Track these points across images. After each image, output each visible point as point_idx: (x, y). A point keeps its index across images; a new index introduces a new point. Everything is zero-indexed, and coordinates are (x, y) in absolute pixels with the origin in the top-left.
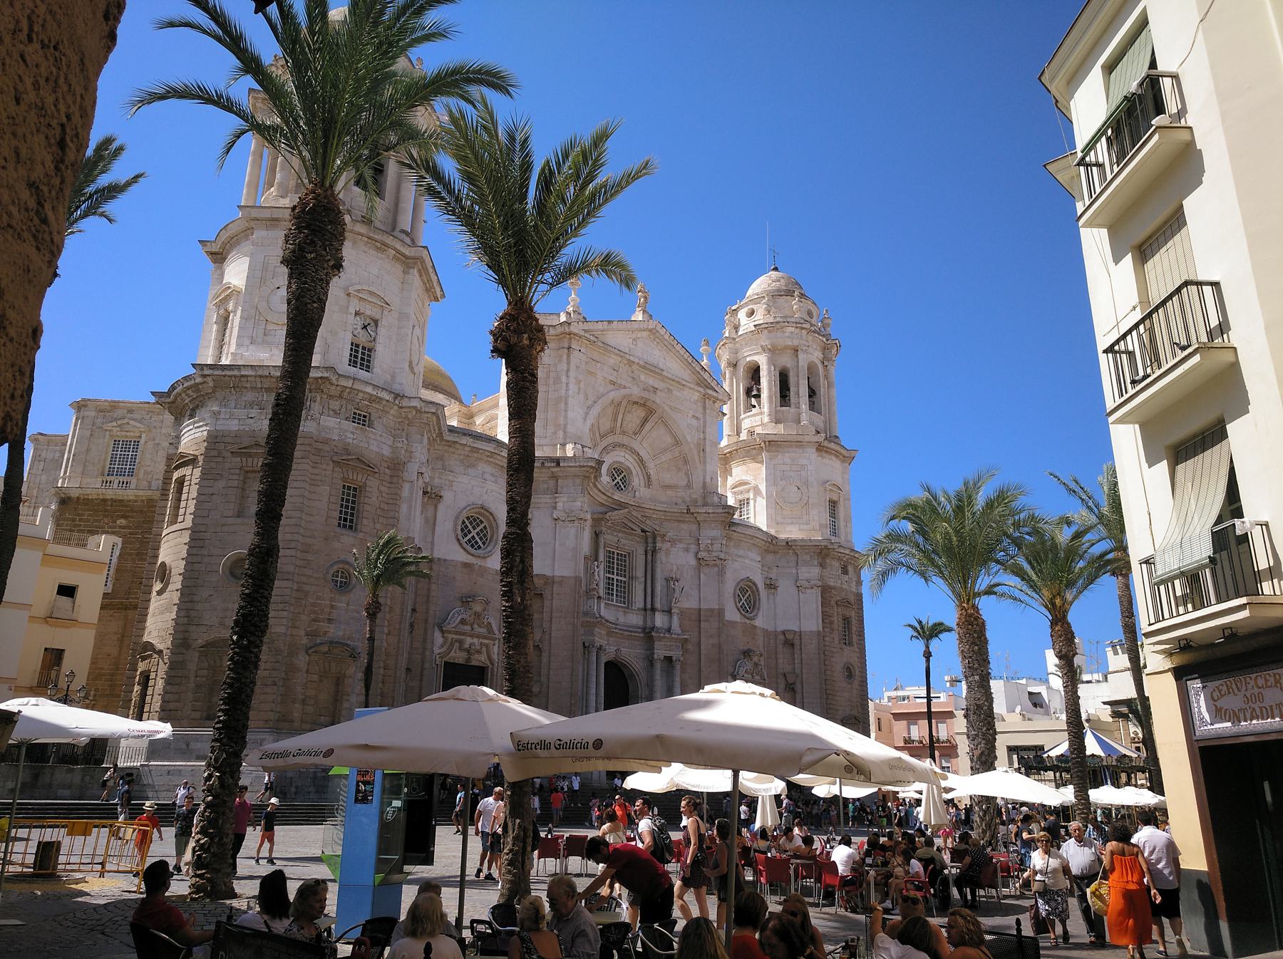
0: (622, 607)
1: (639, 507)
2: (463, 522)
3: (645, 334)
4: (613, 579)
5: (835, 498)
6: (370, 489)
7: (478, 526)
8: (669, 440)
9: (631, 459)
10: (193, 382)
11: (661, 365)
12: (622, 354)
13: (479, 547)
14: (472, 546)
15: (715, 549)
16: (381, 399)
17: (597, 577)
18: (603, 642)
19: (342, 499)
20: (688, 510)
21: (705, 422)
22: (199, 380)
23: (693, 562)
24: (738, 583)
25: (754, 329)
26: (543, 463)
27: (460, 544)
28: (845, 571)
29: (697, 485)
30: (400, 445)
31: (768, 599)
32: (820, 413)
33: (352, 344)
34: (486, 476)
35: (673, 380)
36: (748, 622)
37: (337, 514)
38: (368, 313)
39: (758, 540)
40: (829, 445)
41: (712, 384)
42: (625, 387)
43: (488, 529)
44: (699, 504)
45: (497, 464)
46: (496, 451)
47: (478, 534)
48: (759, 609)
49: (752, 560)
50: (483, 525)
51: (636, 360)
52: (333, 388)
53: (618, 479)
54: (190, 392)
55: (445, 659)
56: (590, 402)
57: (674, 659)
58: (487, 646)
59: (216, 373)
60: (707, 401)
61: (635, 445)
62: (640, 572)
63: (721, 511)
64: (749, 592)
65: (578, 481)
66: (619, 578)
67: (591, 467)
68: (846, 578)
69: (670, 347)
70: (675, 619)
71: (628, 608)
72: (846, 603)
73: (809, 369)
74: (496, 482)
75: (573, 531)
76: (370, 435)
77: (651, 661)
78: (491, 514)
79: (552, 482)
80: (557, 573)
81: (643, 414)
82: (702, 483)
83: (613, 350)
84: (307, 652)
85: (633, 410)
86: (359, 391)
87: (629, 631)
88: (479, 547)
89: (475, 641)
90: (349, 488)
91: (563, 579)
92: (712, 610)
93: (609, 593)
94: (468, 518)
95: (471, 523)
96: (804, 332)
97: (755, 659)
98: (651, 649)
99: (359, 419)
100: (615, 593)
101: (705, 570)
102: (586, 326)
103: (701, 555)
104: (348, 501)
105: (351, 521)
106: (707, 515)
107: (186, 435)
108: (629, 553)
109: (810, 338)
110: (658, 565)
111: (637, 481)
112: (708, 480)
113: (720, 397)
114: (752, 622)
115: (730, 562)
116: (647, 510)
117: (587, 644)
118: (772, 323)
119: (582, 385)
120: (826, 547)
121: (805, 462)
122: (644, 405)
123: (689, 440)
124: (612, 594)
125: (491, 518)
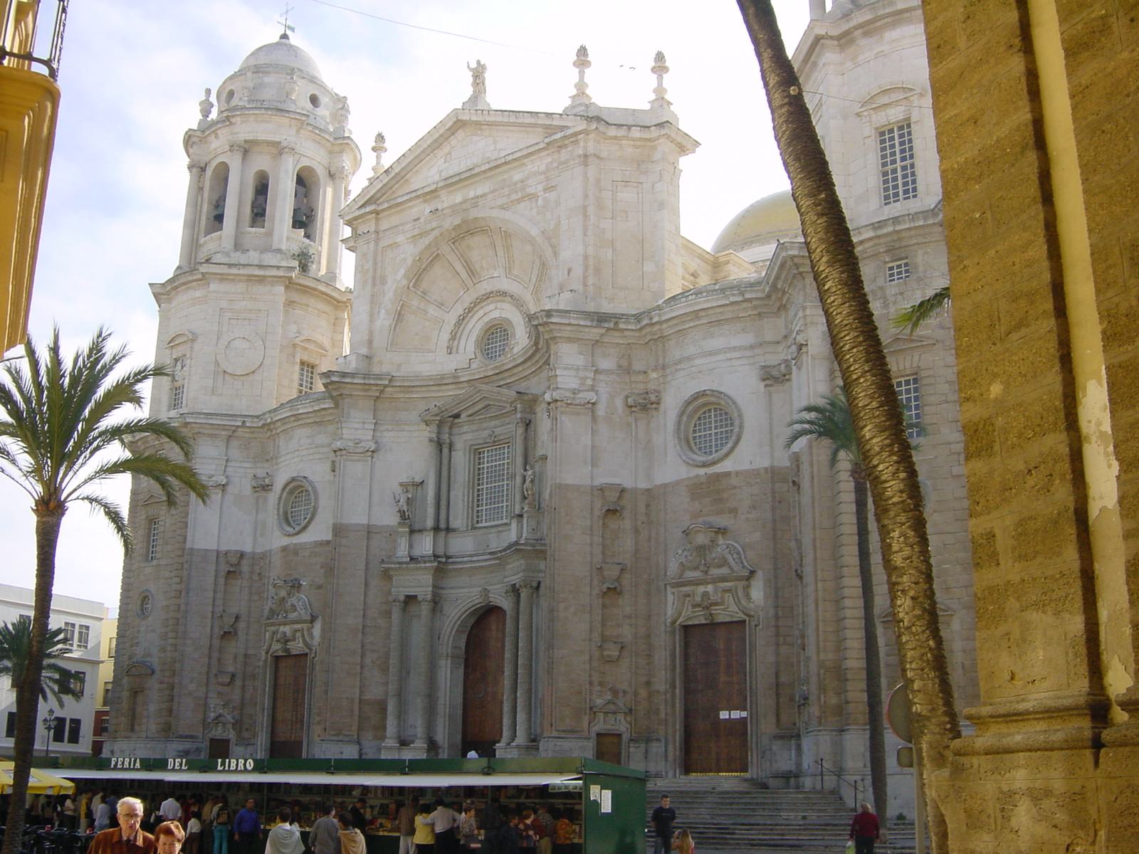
3: (461, 134)
6: (163, 518)
36: (702, 471)
89: (287, 629)
115: (669, 378)
116: (515, 371)
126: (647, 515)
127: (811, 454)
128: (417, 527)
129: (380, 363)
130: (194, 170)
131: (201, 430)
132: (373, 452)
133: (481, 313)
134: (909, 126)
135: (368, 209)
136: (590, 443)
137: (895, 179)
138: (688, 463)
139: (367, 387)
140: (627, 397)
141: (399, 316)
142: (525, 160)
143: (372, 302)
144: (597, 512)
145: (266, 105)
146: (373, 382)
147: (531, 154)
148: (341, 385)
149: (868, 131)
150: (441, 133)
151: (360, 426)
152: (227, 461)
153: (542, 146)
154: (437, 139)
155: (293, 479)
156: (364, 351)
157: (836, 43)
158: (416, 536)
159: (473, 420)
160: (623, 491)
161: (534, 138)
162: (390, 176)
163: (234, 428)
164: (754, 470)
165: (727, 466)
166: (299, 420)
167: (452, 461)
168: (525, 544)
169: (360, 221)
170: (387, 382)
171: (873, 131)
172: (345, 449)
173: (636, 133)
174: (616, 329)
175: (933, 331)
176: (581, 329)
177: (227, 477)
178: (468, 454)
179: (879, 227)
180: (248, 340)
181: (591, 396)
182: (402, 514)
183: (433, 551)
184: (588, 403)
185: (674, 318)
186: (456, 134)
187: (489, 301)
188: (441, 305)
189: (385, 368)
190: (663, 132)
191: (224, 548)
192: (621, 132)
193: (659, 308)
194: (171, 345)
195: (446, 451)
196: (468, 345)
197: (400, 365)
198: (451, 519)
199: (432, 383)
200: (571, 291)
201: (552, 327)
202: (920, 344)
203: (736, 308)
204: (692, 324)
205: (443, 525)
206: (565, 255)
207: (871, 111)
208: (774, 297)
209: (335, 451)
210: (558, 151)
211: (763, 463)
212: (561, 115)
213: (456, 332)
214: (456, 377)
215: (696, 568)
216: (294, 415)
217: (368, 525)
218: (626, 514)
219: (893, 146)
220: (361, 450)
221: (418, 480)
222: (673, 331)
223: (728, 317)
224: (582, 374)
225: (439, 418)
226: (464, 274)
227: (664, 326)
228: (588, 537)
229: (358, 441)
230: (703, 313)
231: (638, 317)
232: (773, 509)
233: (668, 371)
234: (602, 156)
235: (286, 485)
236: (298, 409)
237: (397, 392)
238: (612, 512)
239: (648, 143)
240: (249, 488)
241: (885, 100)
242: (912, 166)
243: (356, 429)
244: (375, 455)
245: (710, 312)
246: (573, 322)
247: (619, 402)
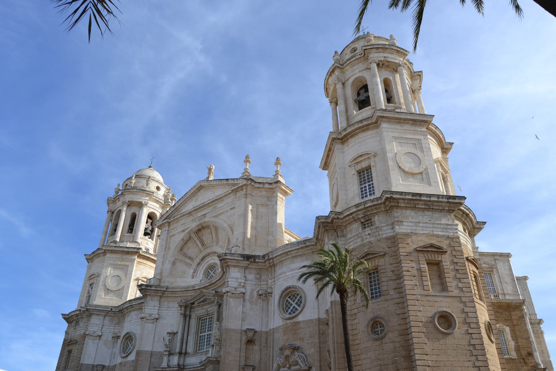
3: (202, 191)
16: (78, 314)
35: (213, 201)
36: (288, 322)
38: (92, 282)
41: (235, 182)
42: (189, 228)
45: (137, 309)
46: (131, 304)
85: (204, 233)
114: (295, 320)
115: (276, 281)
122: (203, 228)
126: (266, 343)
127: (332, 308)
128: (173, 352)
129: (164, 282)
130: (109, 213)
131: (94, 312)
132: (157, 319)
133: (206, 261)
134: (370, 169)
135: (165, 221)
136: (241, 311)
137: (366, 190)
138: (283, 318)
139: (157, 291)
140: (259, 291)
141: (174, 263)
142: (224, 198)
143: (164, 257)
144: (243, 342)
145: (138, 188)
146: (159, 289)
147: (226, 195)
148: (146, 290)
149: (354, 172)
150: (194, 190)
151: (153, 308)
152: (103, 325)
153: (230, 191)
154: (193, 193)
155: (128, 333)
156: (158, 277)
157: (340, 141)
158: (171, 357)
159: (200, 305)
160: (255, 332)
161: (228, 189)
162: (174, 208)
163: (107, 312)
164: (311, 320)
166: (132, 308)
167: (190, 324)
168: (213, 358)
169: (163, 226)
170: (165, 289)
171: (356, 173)
172: (145, 318)
173: (267, 186)
174: (255, 262)
175: (384, 249)
176: (240, 262)
177: (102, 332)
178: (196, 321)
179: (359, 207)
180: (119, 277)
181: (243, 290)
182: (166, 346)
183: (178, 363)
184: (242, 293)
185: (277, 256)
186: (200, 191)
187: (209, 256)
188: (191, 258)
189: (166, 284)
190: (277, 185)
191: (96, 364)
192: (261, 186)
193: (272, 252)
194: (90, 278)
195: (188, 319)
196: (200, 275)
197: (172, 283)
198: (188, 348)
199: (184, 290)
200: (236, 246)
201: (227, 260)
202: (378, 255)
203: (303, 250)
204: (285, 258)
205: (183, 351)
206: (236, 233)
207: (355, 165)
208: (318, 244)
209: (141, 318)
210: (236, 194)
211: (315, 316)
212: (237, 179)
213: (196, 269)
214: (193, 287)
215: (285, 367)
216: (131, 306)
217: (152, 351)
218: (257, 343)
219: (364, 177)
220: (152, 318)
221: (175, 331)
222: (278, 262)
223: (300, 254)
224: (239, 281)
225: (185, 304)
226: (200, 245)
227: (275, 260)
228: (239, 353)
229: (150, 315)
230: (289, 253)
231: (264, 256)
232: (319, 338)
233: (276, 279)
234: (253, 195)
235: (125, 336)
236: (132, 303)
237: (170, 294)
238: (250, 342)
239: (272, 190)
240: (111, 337)
241: (361, 159)
242: (372, 184)
243: (151, 309)
244: (158, 321)
245: (292, 252)
246: (236, 258)
247: (255, 294)
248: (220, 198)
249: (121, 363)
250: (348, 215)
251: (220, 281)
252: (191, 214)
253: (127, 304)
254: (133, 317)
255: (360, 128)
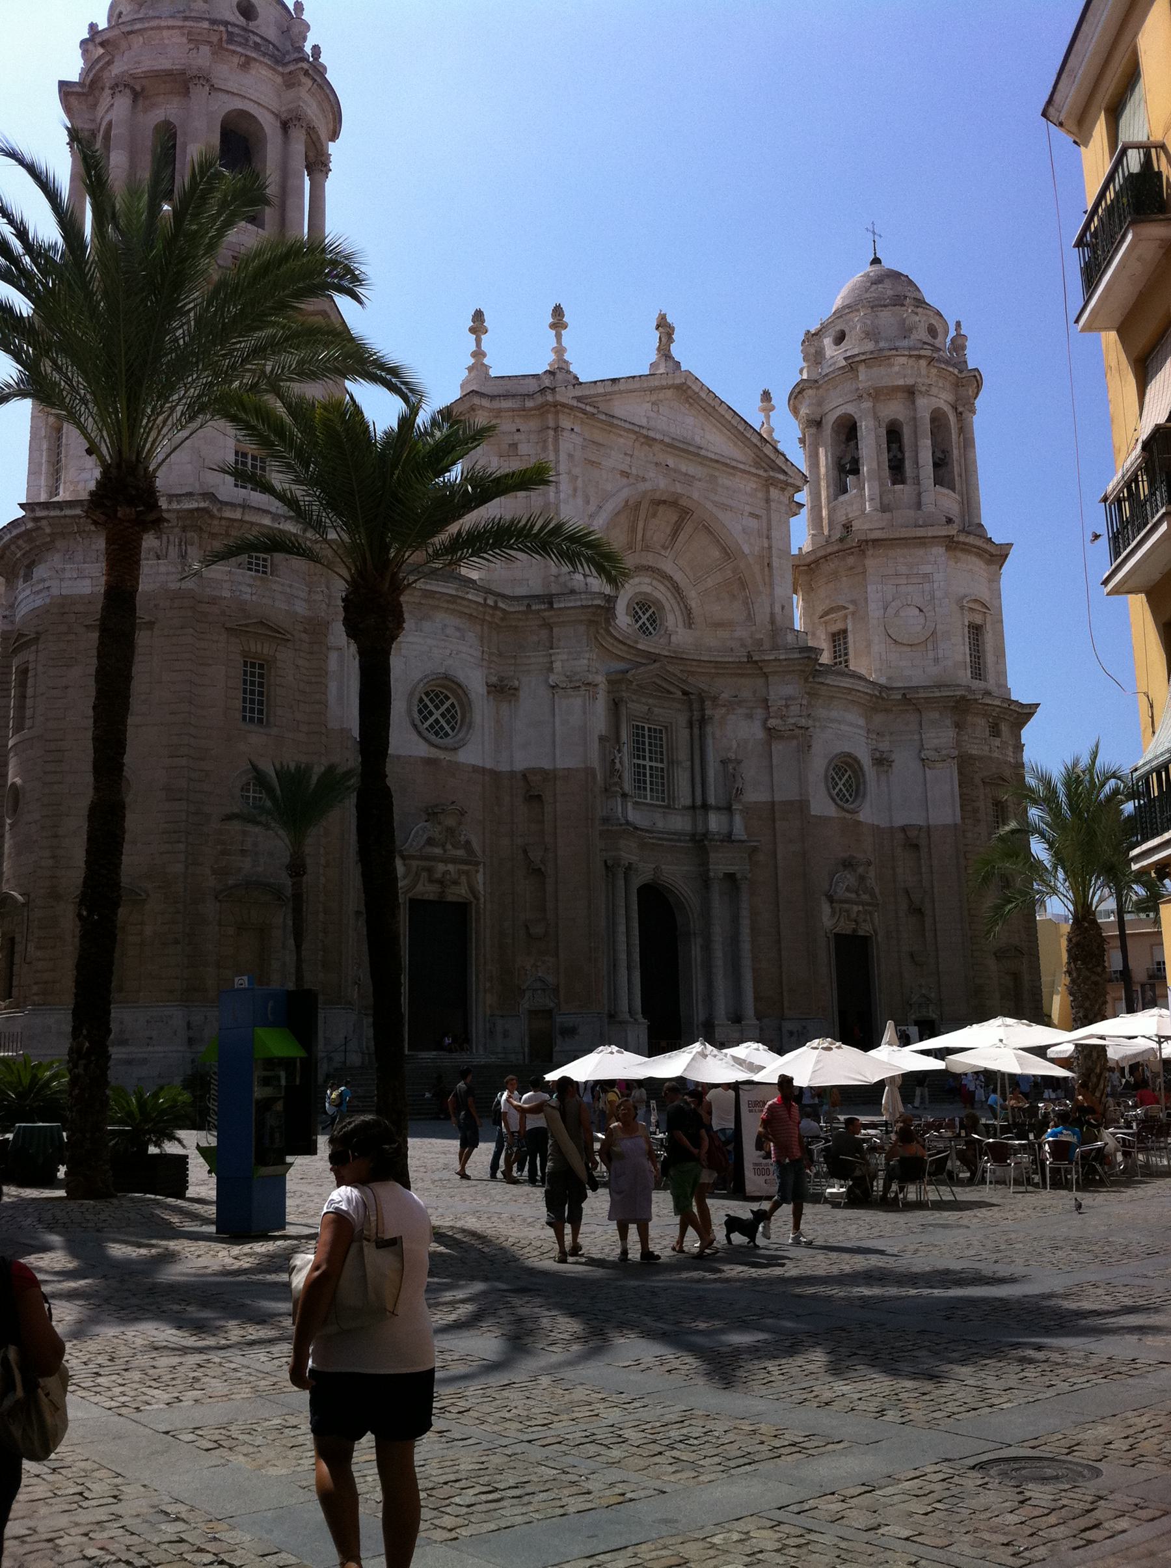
0: (660, 806)
1: (677, 658)
2: (421, 700)
3: (669, 393)
4: (644, 766)
5: (978, 621)
7: (442, 703)
8: (716, 553)
9: (662, 588)
10: (23, 528)
11: (697, 439)
12: (637, 429)
13: (447, 735)
14: (436, 734)
15: (792, 714)
17: (618, 766)
18: (634, 859)
19: (245, 682)
20: (749, 656)
21: (769, 521)
22: (30, 525)
23: (760, 734)
24: (832, 760)
25: (844, 363)
26: (529, 606)
27: (419, 733)
28: (995, 731)
29: (762, 616)
30: (319, 597)
31: (878, 781)
32: (953, 490)
33: (237, 453)
34: (449, 631)
35: (717, 461)
36: (848, 816)
37: (238, 704)
39: (858, 694)
40: (967, 540)
42: (644, 479)
43: (457, 708)
44: (766, 646)
45: (462, 613)
46: (460, 594)
47: (443, 715)
48: (864, 796)
49: (851, 725)
50: (450, 702)
51: (658, 436)
52: (216, 522)
53: (644, 618)
54: (20, 542)
55: (410, 895)
56: (592, 508)
57: (739, 876)
58: (467, 873)
59: (53, 513)
60: (772, 489)
61: (668, 567)
62: (682, 755)
63: (796, 656)
64: (849, 773)
65: (582, 629)
66: (654, 764)
67: (599, 606)
68: (997, 742)
69: (709, 409)
70: (738, 819)
71: (668, 807)
72: (999, 781)
73: (933, 420)
74: (463, 638)
75: (579, 701)
76: (275, 587)
77: (705, 881)
78: (460, 686)
79: (544, 633)
80: (560, 764)
81: (675, 518)
82: (768, 616)
83: (622, 424)
84: (216, 898)
86: (252, 524)
87: (670, 840)
88: (447, 735)
89: (451, 867)
90: (253, 665)
91: (569, 773)
92: (791, 803)
93: (639, 788)
94: (427, 694)
95: (432, 701)
96: (923, 363)
97: (861, 870)
98: (704, 864)
99: (258, 565)
100: (648, 786)
101: (777, 747)
102: (578, 392)
103: (772, 723)
104: (253, 683)
105: (261, 712)
106: (777, 663)
107: (22, 605)
108: (666, 727)
109: (934, 371)
110: (710, 741)
111: (672, 619)
112: (777, 609)
113: (790, 481)
114: (855, 817)
115: (818, 730)
116: (688, 662)
117: (610, 863)
118: (872, 352)
119: (579, 483)
120: (963, 697)
121: (928, 569)
123: (747, 551)
124: (645, 789)
125: (460, 691)
165: (861, 817)
166: (454, 602)
169: (566, 410)
227: (825, 688)
230: (854, 693)
236: (467, 593)
248: (734, 468)
249: (430, 762)
250: (988, 705)
251: (703, 664)
252: (651, 442)
253: (448, 587)
254: (449, 631)
255: (978, 548)
